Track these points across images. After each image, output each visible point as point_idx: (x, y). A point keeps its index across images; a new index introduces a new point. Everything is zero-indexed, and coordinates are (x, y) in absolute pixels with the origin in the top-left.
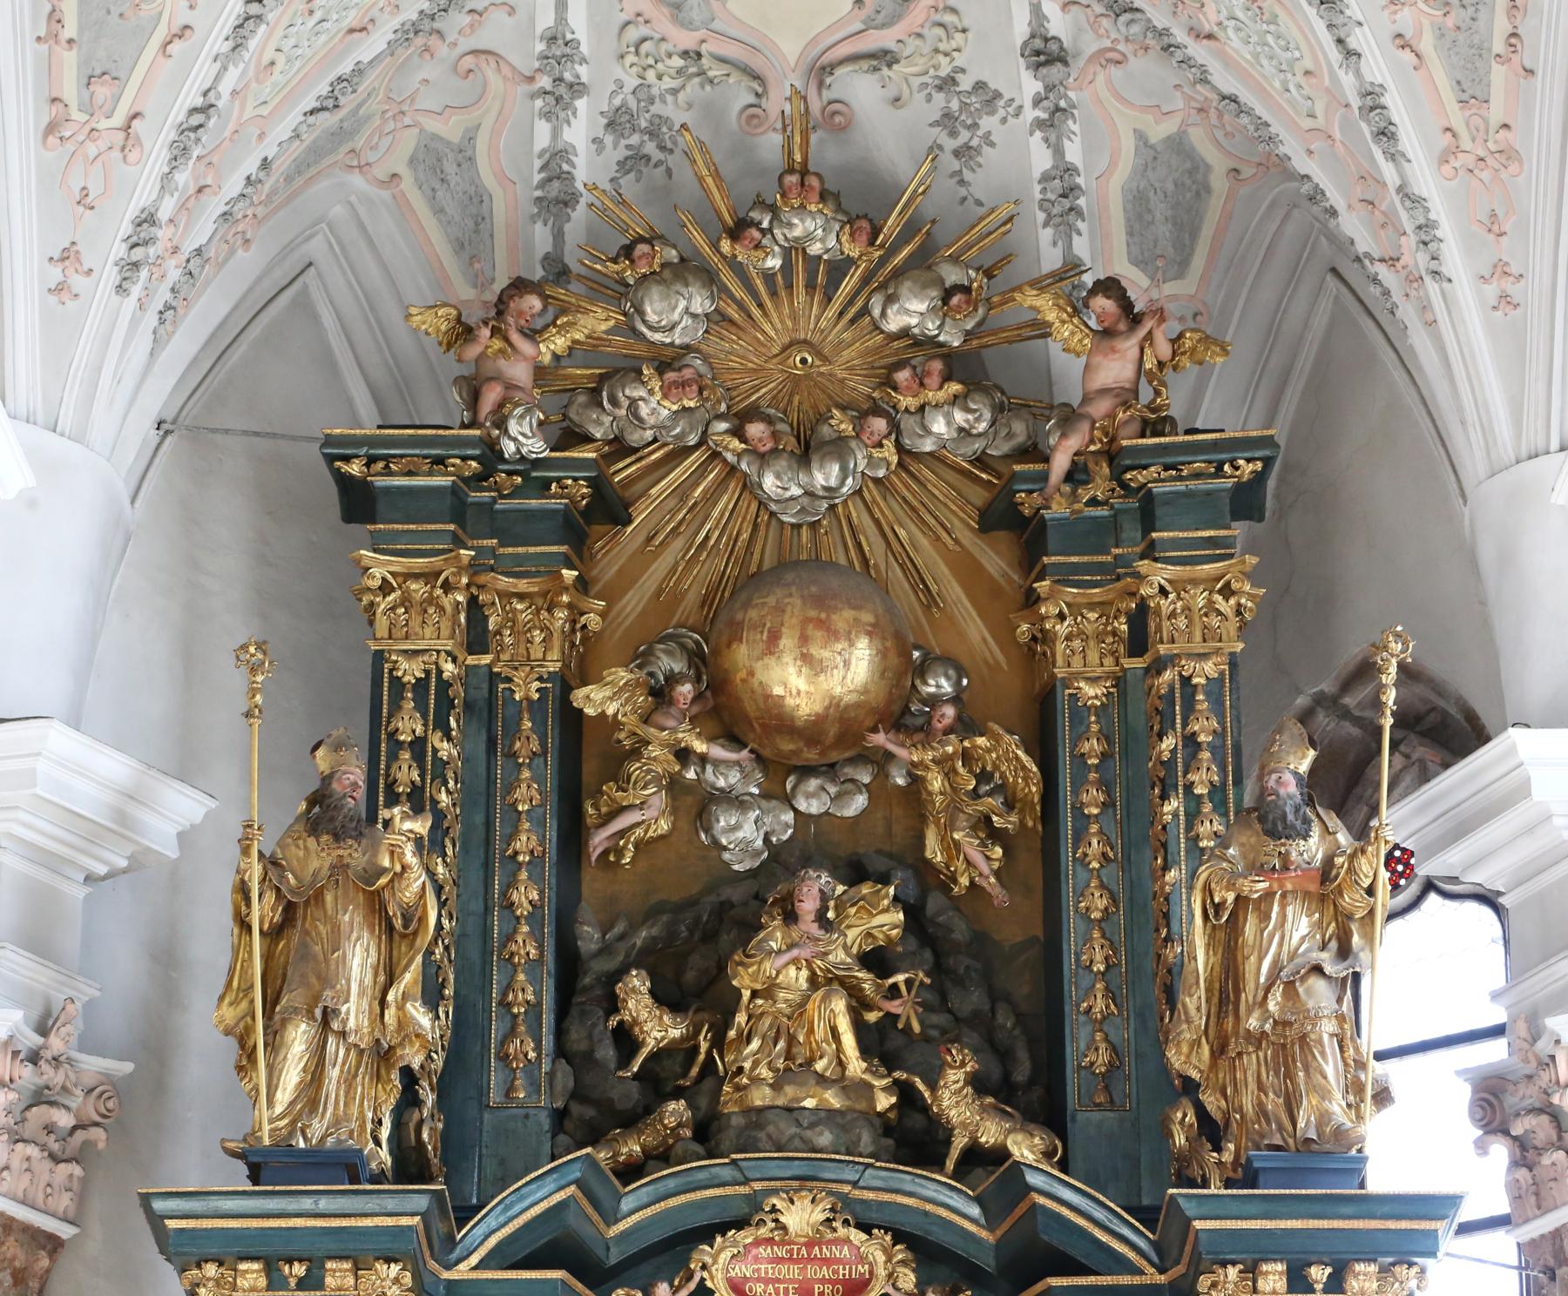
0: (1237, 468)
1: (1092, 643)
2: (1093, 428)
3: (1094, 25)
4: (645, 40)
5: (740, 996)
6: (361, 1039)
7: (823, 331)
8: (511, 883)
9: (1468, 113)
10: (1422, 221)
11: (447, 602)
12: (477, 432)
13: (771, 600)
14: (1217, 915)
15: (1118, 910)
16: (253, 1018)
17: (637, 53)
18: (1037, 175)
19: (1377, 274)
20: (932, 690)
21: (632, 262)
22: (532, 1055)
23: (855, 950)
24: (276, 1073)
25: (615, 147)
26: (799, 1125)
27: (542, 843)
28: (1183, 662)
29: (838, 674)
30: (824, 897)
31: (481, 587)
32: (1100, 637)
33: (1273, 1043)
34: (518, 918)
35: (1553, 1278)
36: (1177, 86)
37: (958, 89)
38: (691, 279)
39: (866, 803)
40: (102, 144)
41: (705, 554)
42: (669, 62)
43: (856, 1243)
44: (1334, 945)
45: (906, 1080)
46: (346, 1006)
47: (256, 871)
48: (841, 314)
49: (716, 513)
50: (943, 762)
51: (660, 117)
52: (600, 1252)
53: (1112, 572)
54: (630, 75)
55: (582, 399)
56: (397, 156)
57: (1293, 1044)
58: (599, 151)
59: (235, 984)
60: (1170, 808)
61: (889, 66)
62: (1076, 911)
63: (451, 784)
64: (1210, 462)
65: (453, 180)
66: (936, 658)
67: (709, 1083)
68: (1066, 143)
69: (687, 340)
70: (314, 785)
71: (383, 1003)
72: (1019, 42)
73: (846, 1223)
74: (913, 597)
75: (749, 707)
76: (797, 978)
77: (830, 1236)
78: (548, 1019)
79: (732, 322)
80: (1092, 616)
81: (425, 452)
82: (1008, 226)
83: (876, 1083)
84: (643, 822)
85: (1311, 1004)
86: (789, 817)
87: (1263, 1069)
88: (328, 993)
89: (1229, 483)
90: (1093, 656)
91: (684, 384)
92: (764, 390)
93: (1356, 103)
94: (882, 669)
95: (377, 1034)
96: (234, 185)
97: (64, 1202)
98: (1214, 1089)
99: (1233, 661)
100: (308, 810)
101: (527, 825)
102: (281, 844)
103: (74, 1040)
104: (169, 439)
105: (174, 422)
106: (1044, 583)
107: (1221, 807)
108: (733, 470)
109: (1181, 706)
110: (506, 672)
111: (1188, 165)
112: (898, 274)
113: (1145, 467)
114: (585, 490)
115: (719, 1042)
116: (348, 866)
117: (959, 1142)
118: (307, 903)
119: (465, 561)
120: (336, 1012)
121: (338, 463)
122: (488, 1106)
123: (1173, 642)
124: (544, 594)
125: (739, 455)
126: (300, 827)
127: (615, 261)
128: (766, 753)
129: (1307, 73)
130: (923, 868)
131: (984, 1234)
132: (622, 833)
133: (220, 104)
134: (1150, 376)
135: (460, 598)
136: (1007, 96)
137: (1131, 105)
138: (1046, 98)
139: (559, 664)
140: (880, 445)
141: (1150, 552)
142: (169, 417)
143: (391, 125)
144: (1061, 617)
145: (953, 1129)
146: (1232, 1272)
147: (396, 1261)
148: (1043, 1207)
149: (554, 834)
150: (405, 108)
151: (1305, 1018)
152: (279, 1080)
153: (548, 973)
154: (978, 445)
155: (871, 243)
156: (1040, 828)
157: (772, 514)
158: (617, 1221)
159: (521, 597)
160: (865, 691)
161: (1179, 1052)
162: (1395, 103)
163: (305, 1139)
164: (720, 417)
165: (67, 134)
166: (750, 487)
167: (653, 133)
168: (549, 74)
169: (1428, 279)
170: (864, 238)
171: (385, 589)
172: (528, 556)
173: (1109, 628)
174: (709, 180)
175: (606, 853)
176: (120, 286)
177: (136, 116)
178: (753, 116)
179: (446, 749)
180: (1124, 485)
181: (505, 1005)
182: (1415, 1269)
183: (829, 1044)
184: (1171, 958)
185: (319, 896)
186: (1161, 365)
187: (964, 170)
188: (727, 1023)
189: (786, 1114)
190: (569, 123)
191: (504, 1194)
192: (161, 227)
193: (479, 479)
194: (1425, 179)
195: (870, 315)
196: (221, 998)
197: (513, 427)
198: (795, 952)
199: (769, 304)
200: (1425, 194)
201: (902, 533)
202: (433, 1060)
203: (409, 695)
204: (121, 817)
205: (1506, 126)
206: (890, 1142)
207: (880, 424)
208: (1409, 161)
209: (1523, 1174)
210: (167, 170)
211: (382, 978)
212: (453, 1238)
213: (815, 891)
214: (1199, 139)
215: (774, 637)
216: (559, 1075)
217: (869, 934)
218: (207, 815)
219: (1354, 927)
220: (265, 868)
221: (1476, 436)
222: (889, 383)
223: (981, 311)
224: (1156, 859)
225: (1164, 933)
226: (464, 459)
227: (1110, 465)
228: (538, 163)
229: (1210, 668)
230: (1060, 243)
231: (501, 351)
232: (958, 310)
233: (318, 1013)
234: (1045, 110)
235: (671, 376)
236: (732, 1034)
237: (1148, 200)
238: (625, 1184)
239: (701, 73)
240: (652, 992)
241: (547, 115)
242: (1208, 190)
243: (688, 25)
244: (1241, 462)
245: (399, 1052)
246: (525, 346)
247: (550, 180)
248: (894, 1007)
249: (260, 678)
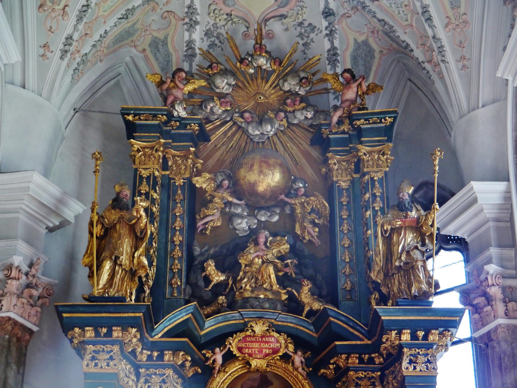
0: (386, 120)
1: (344, 171)
2: (344, 110)
3: (342, 5)
4: (215, 9)
5: (241, 267)
6: (126, 267)
7: (266, 90)
8: (174, 235)
9: (454, 11)
10: (440, 45)
11: (156, 155)
12: (166, 108)
13: (251, 156)
14: (386, 234)
15: (353, 245)
16: (93, 262)
17: (214, 13)
18: (326, 50)
19: (425, 67)
20: (297, 187)
21: (212, 69)
22: (179, 283)
23: (275, 255)
24: (100, 276)
25: (207, 41)
26: (259, 302)
27: (183, 224)
28: (371, 173)
29: (270, 177)
30: (267, 239)
31: (167, 153)
32: (346, 170)
33: (403, 270)
34: (176, 245)
35: (487, 346)
36: (366, 25)
37: (304, 26)
38: (228, 74)
39: (278, 218)
40: (57, 13)
41: (232, 149)
42: (222, 16)
43: (276, 337)
44: (420, 243)
45: (291, 291)
46: (122, 257)
47: (96, 218)
48: (271, 86)
49: (235, 139)
50: (302, 204)
51: (220, 33)
52: (199, 339)
53: (349, 152)
54: (211, 20)
55: (197, 107)
56: (145, 42)
57: (409, 270)
58: (203, 42)
59: (89, 252)
60: (368, 213)
61: (285, 18)
62: (340, 245)
63: (157, 206)
64: (378, 118)
65: (161, 50)
66: (298, 178)
67: (232, 293)
68: (334, 40)
69: (227, 92)
70: (114, 196)
71: (133, 257)
72: (321, 10)
73: (273, 331)
74: (291, 162)
75: (245, 187)
76: (259, 261)
77: (268, 334)
78: (184, 273)
79: (240, 87)
80: (344, 164)
81: (150, 112)
82: (318, 62)
83: (281, 291)
84: (213, 220)
85: (415, 257)
86: (256, 221)
87: (400, 278)
88: (116, 252)
89: (383, 125)
90: (344, 175)
91: (227, 102)
92: (249, 106)
93: (420, 11)
95: (132, 266)
96: (97, 37)
97: (34, 319)
98: (384, 286)
99: (386, 173)
100: (113, 203)
101: (179, 219)
102: (104, 212)
103: (40, 271)
104: (77, 114)
105: (79, 109)
106: (330, 154)
107: (383, 213)
108: (240, 127)
109: (371, 186)
110: (173, 177)
111: (368, 49)
112: (287, 75)
113: (359, 120)
114: (197, 128)
115: (235, 282)
116: (124, 217)
117: (307, 309)
118: (111, 228)
119: (162, 143)
120: (119, 258)
121: (126, 116)
122: (166, 298)
123: (368, 168)
124: (185, 156)
125: (242, 123)
126: (110, 207)
127: (207, 69)
128: (250, 203)
129: (406, 6)
130: (296, 237)
131: (315, 335)
132: (206, 223)
133: (93, 5)
134: (360, 96)
135: (160, 154)
136: (318, 27)
137: (353, 31)
138: (329, 27)
139: (189, 175)
140: (282, 120)
141: (361, 143)
142: (77, 106)
143: (143, 34)
144: (335, 164)
145: (305, 305)
146: (394, 333)
147: (135, 328)
148: (333, 322)
149: (187, 222)
150: (148, 28)
151: (413, 261)
152: (101, 277)
153: (184, 261)
154: (310, 122)
155: (280, 65)
156: (329, 225)
157: (251, 139)
158: (203, 330)
159: (178, 156)
160: (278, 183)
161: (374, 275)
162: (432, 11)
163: (108, 294)
165: (46, 9)
166: (245, 132)
167: (218, 38)
168: (189, 18)
169: (441, 64)
170: (278, 63)
171: (138, 151)
172: (180, 146)
173: (349, 167)
174: (234, 48)
175: (202, 230)
176: (61, 57)
177: (66, 6)
178: (246, 34)
179: (155, 196)
180: (353, 127)
181: (171, 269)
182: (450, 333)
183: (267, 279)
184: (369, 255)
185: (115, 225)
186: (363, 93)
187: (306, 50)
188: (238, 275)
189: (255, 299)
190: (194, 33)
191: (169, 315)
192: (74, 41)
193: (166, 123)
195: (279, 85)
196: (84, 256)
197: (177, 107)
198: (258, 253)
199: (250, 82)
200: (441, 38)
201: (288, 145)
202: (149, 282)
203: (145, 180)
204: (57, 207)
205: (465, 14)
206: (286, 308)
207: (282, 114)
208: (436, 27)
209: (476, 316)
210: (76, 23)
211: (133, 250)
212: (153, 327)
213: (264, 236)
214: (371, 41)
215: (252, 166)
216: (187, 289)
217: (279, 251)
218: (83, 211)
219: (426, 238)
220: (99, 217)
221: (456, 109)
222: (285, 103)
223: (311, 85)
224: (364, 228)
225: (367, 249)
226: (162, 115)
227: (349, 120)
228: (185, 44)
229: (380, 175)
230: (333, 70)
231: (174, 87)
232: (304, 84)
233: (113, 257)
234: (328, 30)
235: (222, 100)
236: (239, 278)
237: (357, 59)
238: (206, 318)
239: (232, 20)
240: (215, 266)
241: (188, 30)
242: (374, 57)
243: (228, 6)
244: (387, 118)
245: (138, 272)
247: (188, 49)
248: (287, 270)
249: (99, 162)
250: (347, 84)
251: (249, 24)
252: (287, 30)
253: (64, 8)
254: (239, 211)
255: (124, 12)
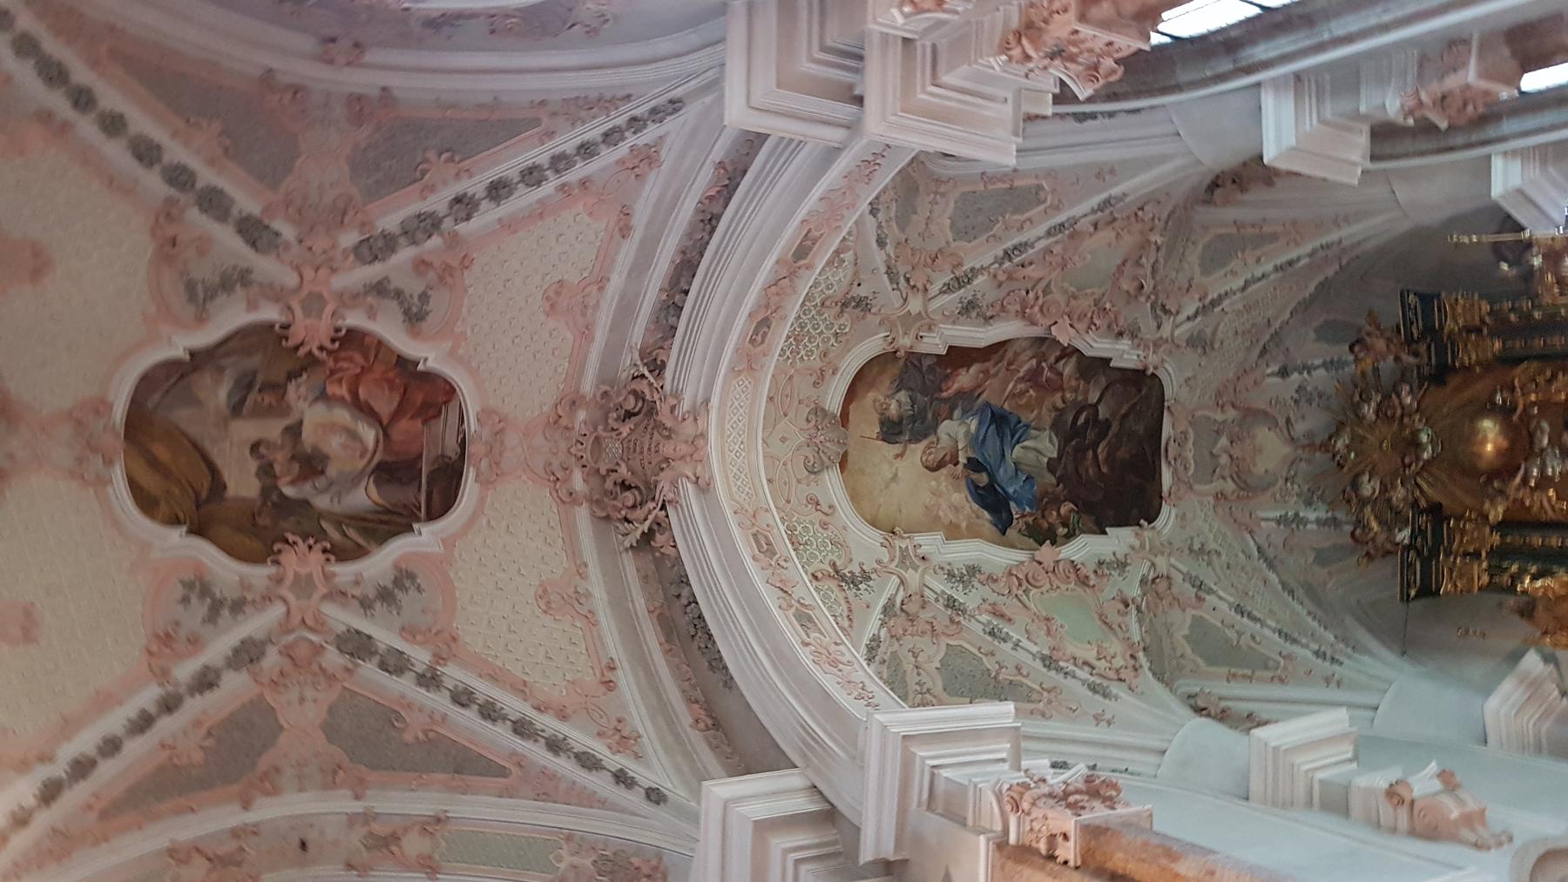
93: (1280, 274)
94: (1487, 417)
96: (1315, 624)
112: (1357, 416)
113: (1412, 334)
133: (1279, 627)
141: (1442, 327)
164: (1404, 471)
177: (1280, 653)
179: (1514, 568)
193: (1419, 553)
194: (1307, 248)
207: (1406, 420)
214: (1316, 324)
241: (1305, 525)
243: (1277, 480)
246: (1372, 534)
250: (1367, 348)
251: (1295, 460)
252: (1303, 417)
253: (1284, 658)
254: (1535, 472)
255: (1286, 594)
